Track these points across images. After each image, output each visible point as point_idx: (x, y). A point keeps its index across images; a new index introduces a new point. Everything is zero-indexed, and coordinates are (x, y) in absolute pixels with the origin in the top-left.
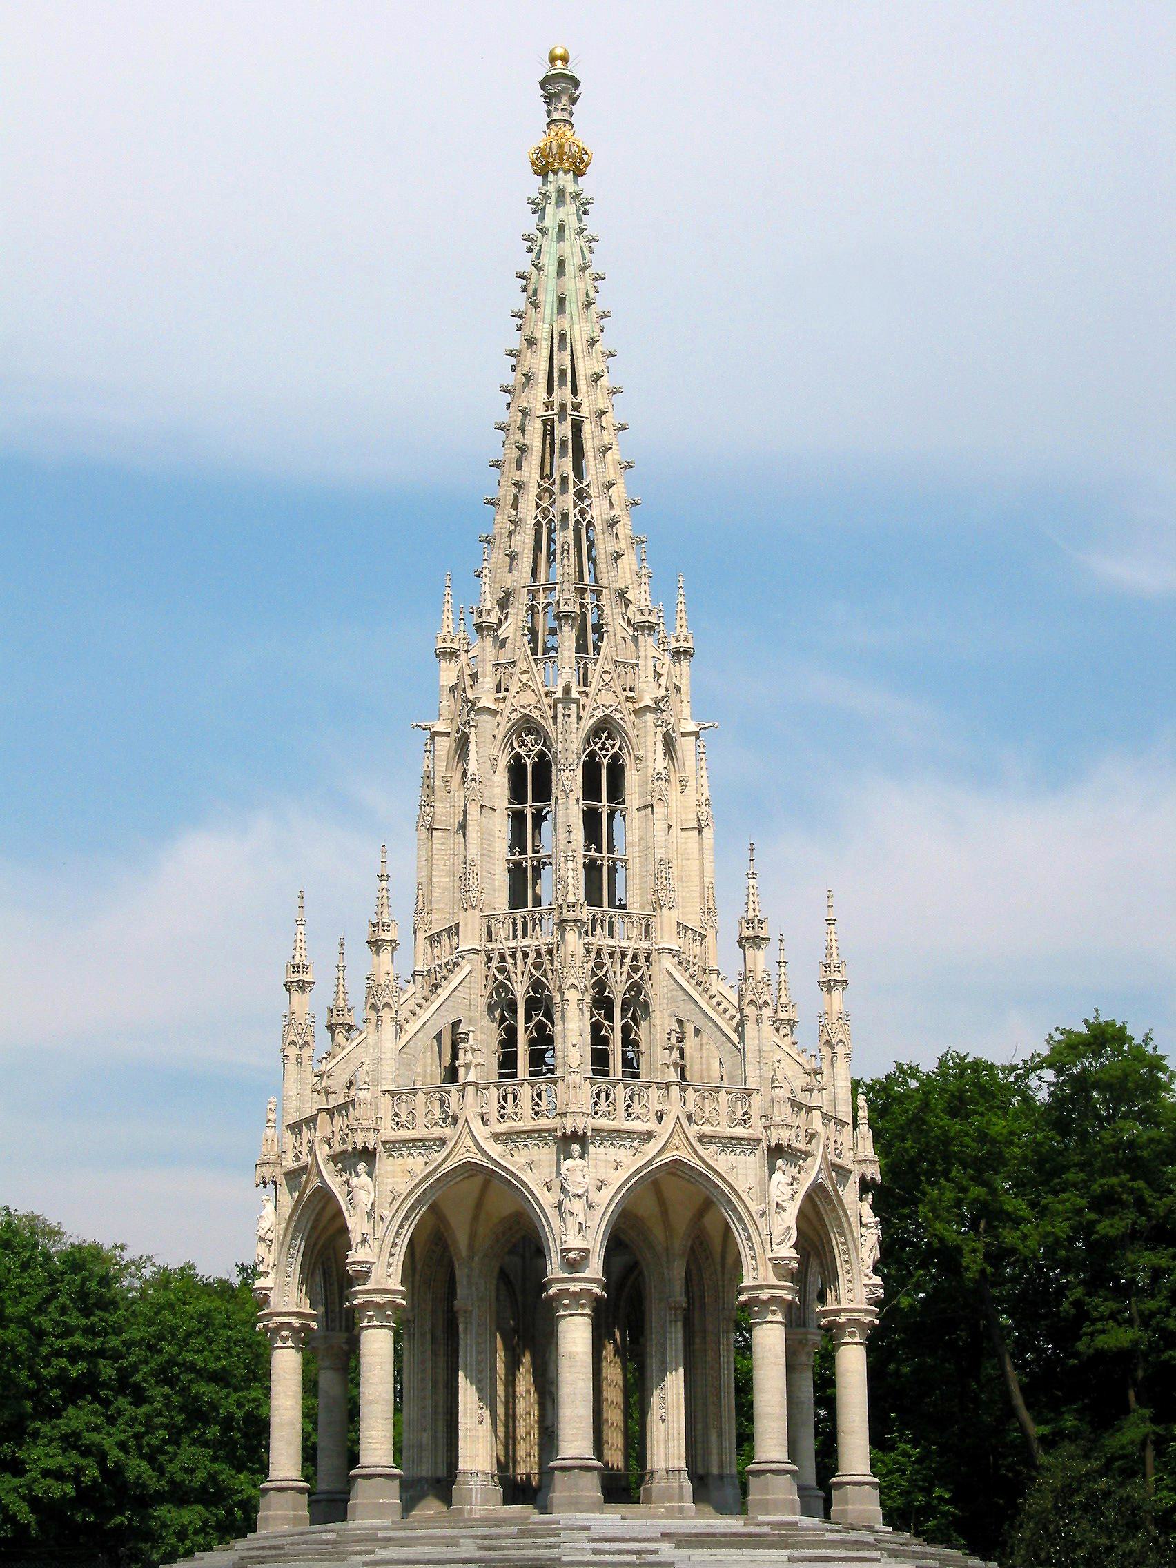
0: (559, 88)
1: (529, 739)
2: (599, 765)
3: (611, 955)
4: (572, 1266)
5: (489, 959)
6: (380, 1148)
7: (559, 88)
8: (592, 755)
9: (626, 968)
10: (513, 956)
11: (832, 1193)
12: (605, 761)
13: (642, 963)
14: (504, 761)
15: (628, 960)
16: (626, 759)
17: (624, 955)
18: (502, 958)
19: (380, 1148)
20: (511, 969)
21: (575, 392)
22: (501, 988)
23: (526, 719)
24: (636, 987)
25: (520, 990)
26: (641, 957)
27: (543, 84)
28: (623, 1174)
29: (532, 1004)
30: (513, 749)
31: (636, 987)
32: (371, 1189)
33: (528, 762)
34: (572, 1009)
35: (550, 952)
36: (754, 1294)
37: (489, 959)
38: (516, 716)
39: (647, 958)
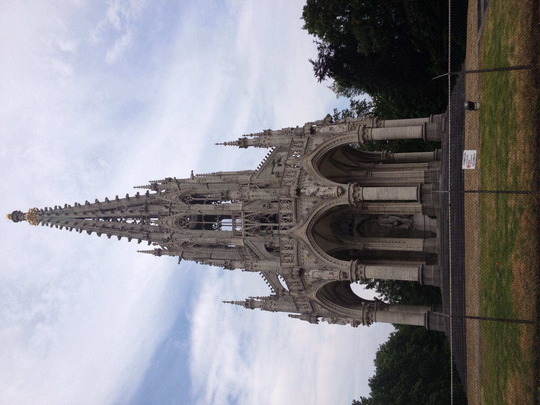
0: (16, 216)
1: (183, 222)
2: (194, 201)
5: (247, 235)
6: (300, 267)
8: (190, 202)
10: (247, 227)
12: (193, 198)
16: (193, 193)
18: (247, 231)
19: (300, 267)
20: (251, 227)
22: (257, 230)
23: (176, 223)
25: (257, 224)
27: (15, 221)
29: (262, 221)
30: (185, 228)
32: (314, 270)
34: (255, 194)
35: (246, 214)
36: (361, 138)
37: (247, 235)
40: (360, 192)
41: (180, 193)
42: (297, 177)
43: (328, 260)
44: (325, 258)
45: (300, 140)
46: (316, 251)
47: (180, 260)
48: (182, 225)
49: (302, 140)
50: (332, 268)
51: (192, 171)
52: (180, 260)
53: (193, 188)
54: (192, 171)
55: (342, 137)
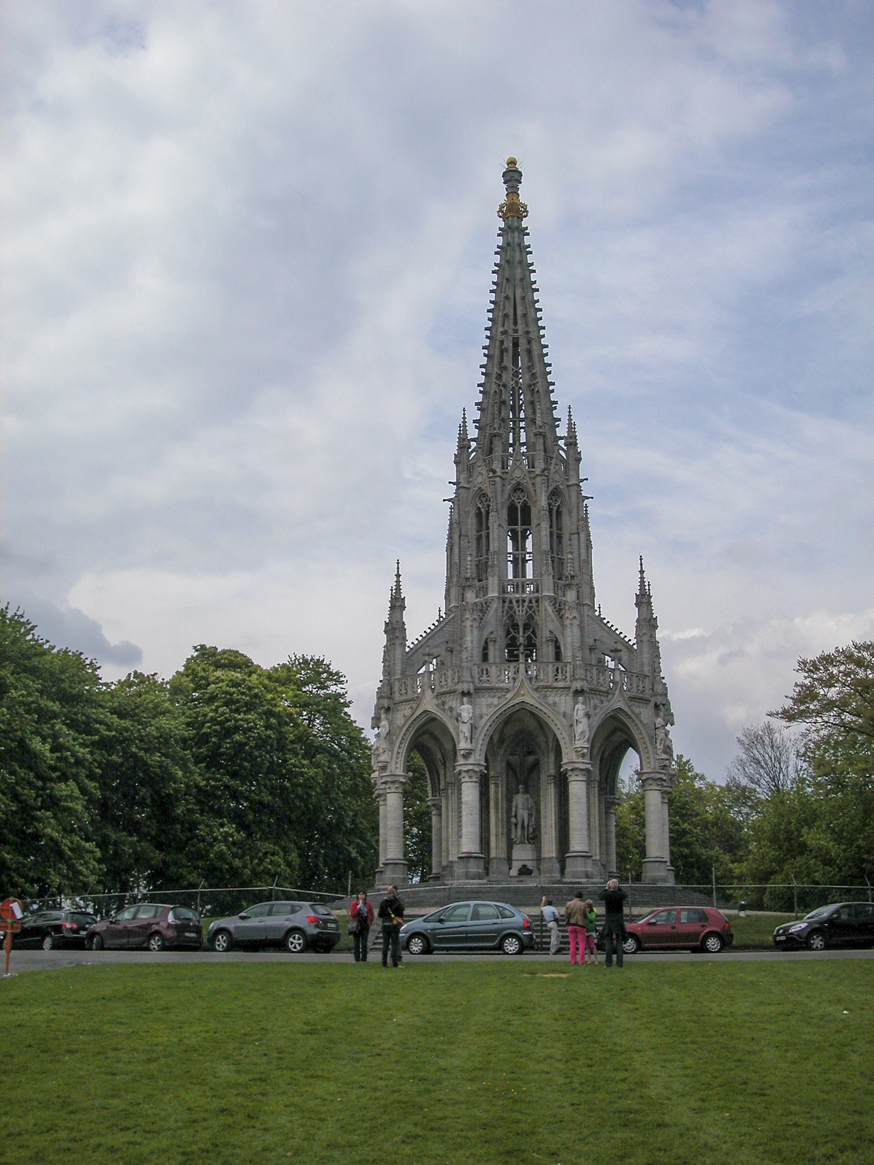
0: (512, 177)
2: (517, 508)
3: (517, 601)
4: (466, 756)
7: (512, 177)
9: (525, 607)
11: (630, 713)
12: (519, 506)
13: (534, 604)
14: (473, 511)
15: (526, 604)
16: (530, 503)
17: (524, 601)
21: (515, 323)
24: (530, 617)
26: (533, 601)
28: (492, 710)
31: (530, 617)
32: (387, 726)
33: (483, 510)
34: (468, 629)
38: (476, 489)
39: (537, 601)
40: (467, 779)
41: (527, 482)
42: (497, 685)
43: (401, 743)
44: (403, 739)
45: (568, 675)
46: (409, 727)
47: (449, 500)
48: (480, 498)
49: (568, 678)
50: (392, 751)
51: (587, 479)
52: (449, 500)
53: (536, 501)
54: (587, 479)
55: (567, 738)
